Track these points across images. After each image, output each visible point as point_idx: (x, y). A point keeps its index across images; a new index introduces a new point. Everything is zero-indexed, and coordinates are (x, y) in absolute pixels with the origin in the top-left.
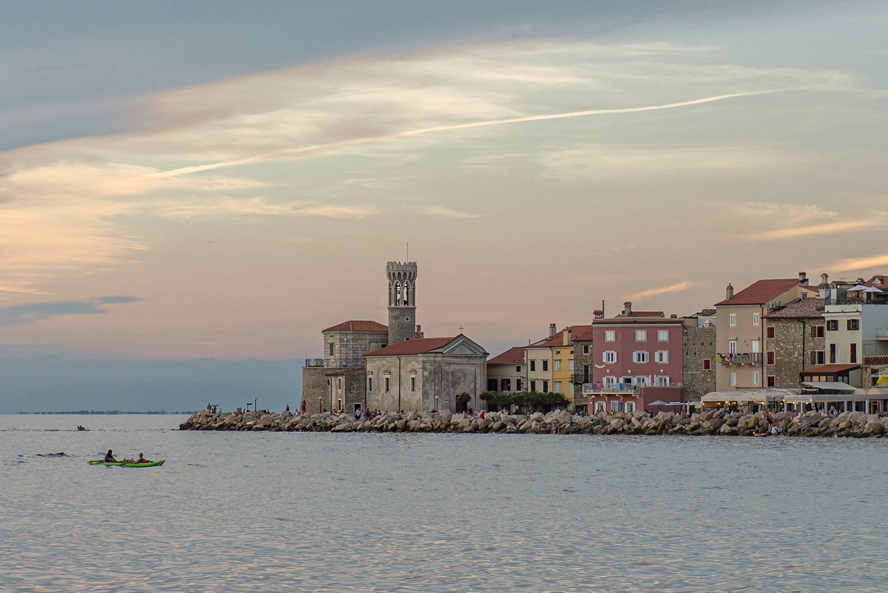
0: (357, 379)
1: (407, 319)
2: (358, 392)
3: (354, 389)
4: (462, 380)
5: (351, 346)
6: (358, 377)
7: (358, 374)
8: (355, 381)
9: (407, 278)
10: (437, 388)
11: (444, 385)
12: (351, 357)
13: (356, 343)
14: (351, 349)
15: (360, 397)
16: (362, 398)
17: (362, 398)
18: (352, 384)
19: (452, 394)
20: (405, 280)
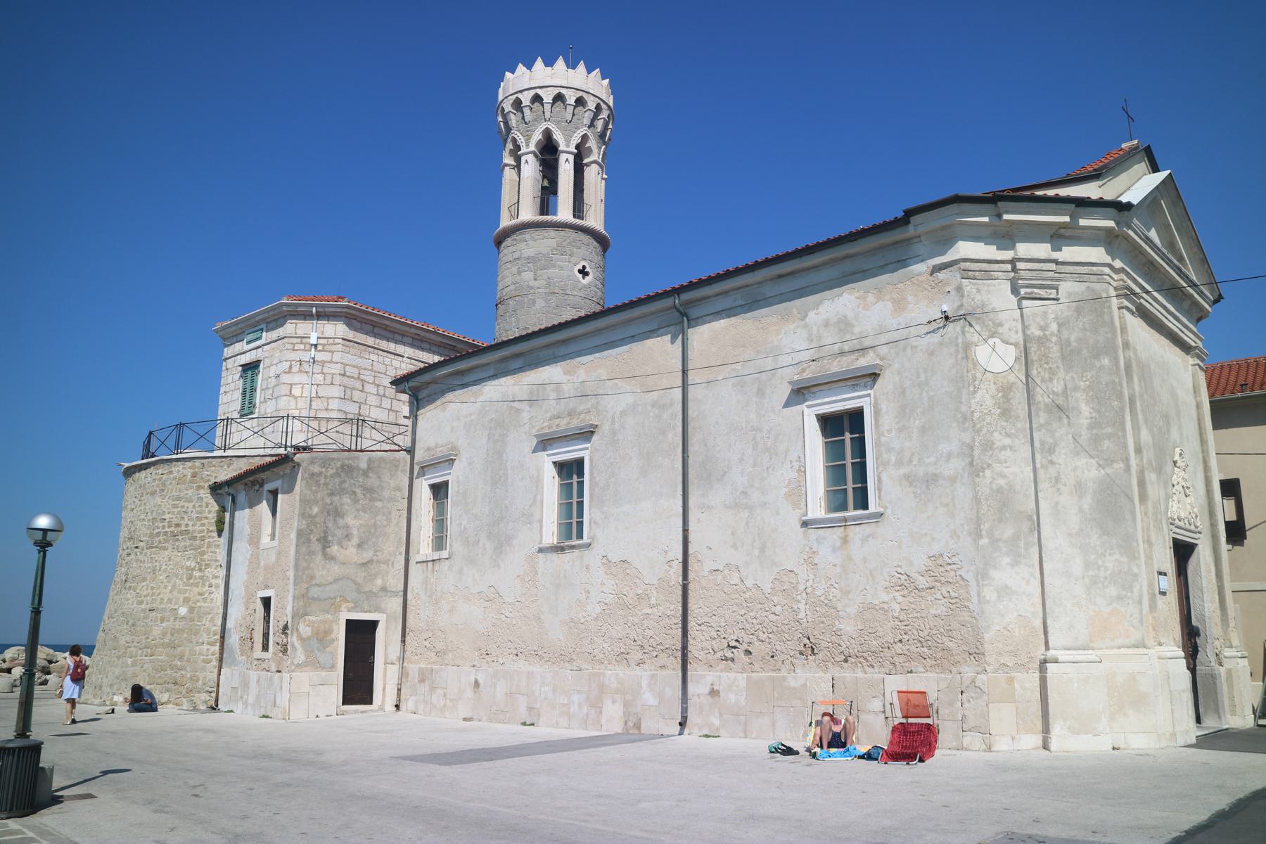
0: (369, 490)
1: (583, 272)
3: (348, 537)
5: (337, 369)
6: (372, 481)
7: (370, 461)
8: (356, 501)
12: (335, 415)
13: (361, 362)
14: (337, 379)
15: (379, 582)
16: (384, 589)
17: (384, 589)
18: (337, 513)
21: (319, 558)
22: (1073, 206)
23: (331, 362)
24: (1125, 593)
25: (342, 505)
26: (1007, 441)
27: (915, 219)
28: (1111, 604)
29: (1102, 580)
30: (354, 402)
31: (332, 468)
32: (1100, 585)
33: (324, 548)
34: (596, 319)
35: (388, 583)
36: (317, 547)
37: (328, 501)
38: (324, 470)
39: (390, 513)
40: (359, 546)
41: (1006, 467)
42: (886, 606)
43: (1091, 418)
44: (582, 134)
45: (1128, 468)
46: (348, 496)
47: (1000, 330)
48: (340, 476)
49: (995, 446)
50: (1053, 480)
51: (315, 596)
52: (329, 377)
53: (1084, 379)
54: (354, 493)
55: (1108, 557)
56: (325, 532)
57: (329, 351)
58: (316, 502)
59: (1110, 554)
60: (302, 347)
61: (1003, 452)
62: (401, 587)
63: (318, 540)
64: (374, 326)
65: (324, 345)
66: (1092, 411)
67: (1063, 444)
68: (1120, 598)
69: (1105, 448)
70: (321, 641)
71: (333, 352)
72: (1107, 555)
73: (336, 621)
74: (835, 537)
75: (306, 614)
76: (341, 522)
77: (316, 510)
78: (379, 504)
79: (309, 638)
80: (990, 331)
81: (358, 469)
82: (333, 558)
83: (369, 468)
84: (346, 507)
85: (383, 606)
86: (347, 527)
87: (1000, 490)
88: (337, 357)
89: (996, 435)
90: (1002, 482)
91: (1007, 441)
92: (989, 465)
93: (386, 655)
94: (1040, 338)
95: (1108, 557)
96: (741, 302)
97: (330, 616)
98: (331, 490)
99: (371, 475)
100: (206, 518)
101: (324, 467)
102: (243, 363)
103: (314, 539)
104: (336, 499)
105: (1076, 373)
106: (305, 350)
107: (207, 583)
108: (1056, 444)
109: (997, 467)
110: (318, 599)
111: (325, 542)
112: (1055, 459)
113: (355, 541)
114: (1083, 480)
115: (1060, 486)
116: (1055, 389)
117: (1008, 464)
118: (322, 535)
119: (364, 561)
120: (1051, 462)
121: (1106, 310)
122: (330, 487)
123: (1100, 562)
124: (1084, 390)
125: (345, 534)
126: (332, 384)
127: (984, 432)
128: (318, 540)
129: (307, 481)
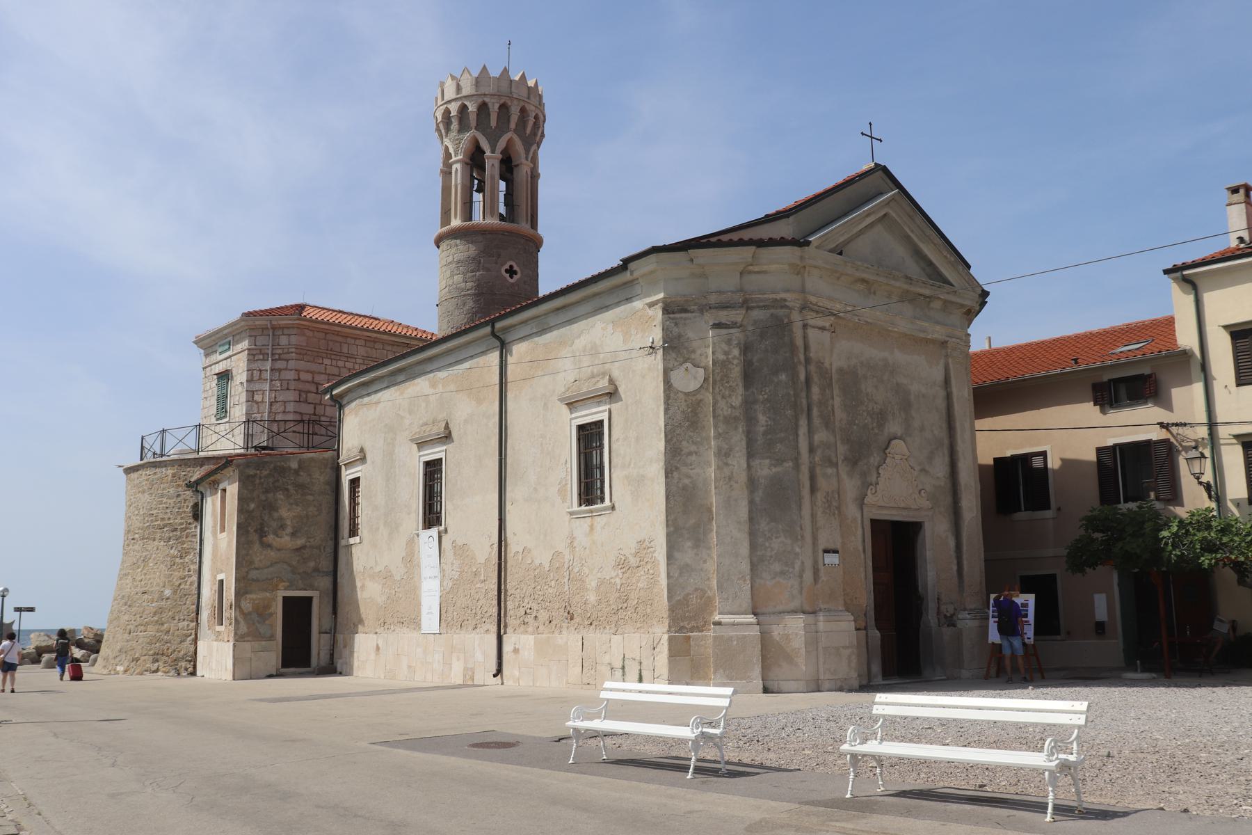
0: (301, 487)
1: (511, 272)
2: (300, 542)
3: (283, 527)
4: (894, 427)
5: (291, 375)
6: (303, 478)
7: (301, 462)
8: (288, 496)
9: (513, 125)
10: (765, 469)
11: (812, 450)
12: (291, 417)
13: (313, 367)
14: (293, 385)
15: (312, 564)
16: (316, 570)
18: (271, 507)
19: (852, 511)
20: (504, 133)
21: (257, 546)
22: (754, 247)
23: (286, 369)
24: (787, 569)
25: (276, 500)
26: (693, 448)
27: (632, 266)
28: (774, 578)
29: (768, 558)
30: (309, 403)
31: (266, 470)
32: (766, 563)
33: (261, 537)
34: (512, 316)
35: (320, 565)
36: (255, 537)
37: (263, 498)
38: (258, 472)
39: (321, 505)
40: (293, 535)
41: (691, 469)
42: (613, 581)
43: (767, 426)
44: (507, 139)
45: (797, 467)
46: (281, 492)
47: (693, 356)
48: (273, 476)
49: (683, 453)
50: (727, 480)
51: (254, 577)
52: (285, 383)
53: (763, 393)
54: (287, 490)
55: (774, 540)
56: (262, 524)
57: (285, 360)
58: (252, 500)
59: (776, 538)
60: (261, 357)
61: (689, 457)
62: (331, 568)
63: (255, 531)
64: (326, 333)
65: (280, 354)
66: (768, 419)
67: (737, 449)
68: (783, 573)
69: (777, 450)
70: (260, 615)
71: (287, 360)
72: (774, 538)
73: (274, 599)
74: (586, 525)
75: (247, 593)
76: (275, 515)
77: (252, 506)
78: (310, 498)
79: (250, 613)
80: (684, 357)
81: (290, 468)
82: (269, 546)
83: (300, 467)
84: (280, 502)
85: (316, 584)
86: (281, 519)
87: (685, 488)
88: (292, 364)
89: (684, 443)
90: (687, 481)
91: (693, 448)
92: (677, 468)
93: (320, 626)
94: (724, 361)
95: (774, 540)
96: (535, 330)
97: (268, 594)
98: (265, 488)
99: (302, 473)
100: (185, 512)
101: (258, 470)
102: (217, 372)
103: (252, 531)
104: (270, 495)
105: (756, 389)
106: (263, 360)
107: (187, 569)
108: (731, 449)
109: (684, 470)
110: (257, 580)
111: (261, 533)
112: (730, 462)
113: (289, 530)
114: (756, 478)
115: (732, 483)
116: (734, 404)
117: (693, 467)
118: (259, 527)
119: (298, 547)
120: (727, 464)
121: (786, 333)
122: (264, 486)
123: (767, 544)
124: (762, 403)
125: (280, 525)
126: (288, 389)
127: (673, 442)
128: (255, 531)
129: (244, 483)
